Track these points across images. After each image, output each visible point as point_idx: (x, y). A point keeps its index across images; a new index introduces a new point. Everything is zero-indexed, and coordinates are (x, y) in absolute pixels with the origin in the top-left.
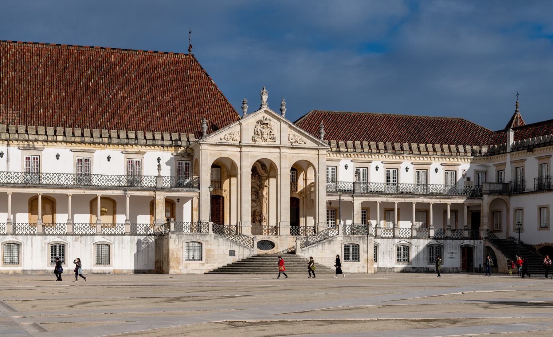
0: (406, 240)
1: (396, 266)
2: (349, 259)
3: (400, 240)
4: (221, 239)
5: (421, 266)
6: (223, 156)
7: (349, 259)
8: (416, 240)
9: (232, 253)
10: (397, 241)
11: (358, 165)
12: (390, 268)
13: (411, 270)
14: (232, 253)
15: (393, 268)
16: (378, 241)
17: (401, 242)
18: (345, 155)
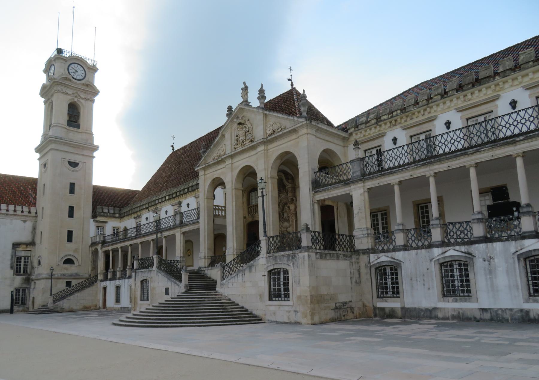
0: (457, 248)
1: (441, 305)
2: (279, 296)
3: (445, 249)
4: (160, 275)
5: (504, 307)
6: (215, 177)
7: (279, 296)
8: (482, 246)
9: (167, 292)
10: (437, 252)
11: (413, 131)
12: (427, 310)
13: (478, 315)
14: (167, 292)
15: (435, 309)
16: (399, 255)
17: (447, 254)
18: (388, 124)
